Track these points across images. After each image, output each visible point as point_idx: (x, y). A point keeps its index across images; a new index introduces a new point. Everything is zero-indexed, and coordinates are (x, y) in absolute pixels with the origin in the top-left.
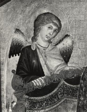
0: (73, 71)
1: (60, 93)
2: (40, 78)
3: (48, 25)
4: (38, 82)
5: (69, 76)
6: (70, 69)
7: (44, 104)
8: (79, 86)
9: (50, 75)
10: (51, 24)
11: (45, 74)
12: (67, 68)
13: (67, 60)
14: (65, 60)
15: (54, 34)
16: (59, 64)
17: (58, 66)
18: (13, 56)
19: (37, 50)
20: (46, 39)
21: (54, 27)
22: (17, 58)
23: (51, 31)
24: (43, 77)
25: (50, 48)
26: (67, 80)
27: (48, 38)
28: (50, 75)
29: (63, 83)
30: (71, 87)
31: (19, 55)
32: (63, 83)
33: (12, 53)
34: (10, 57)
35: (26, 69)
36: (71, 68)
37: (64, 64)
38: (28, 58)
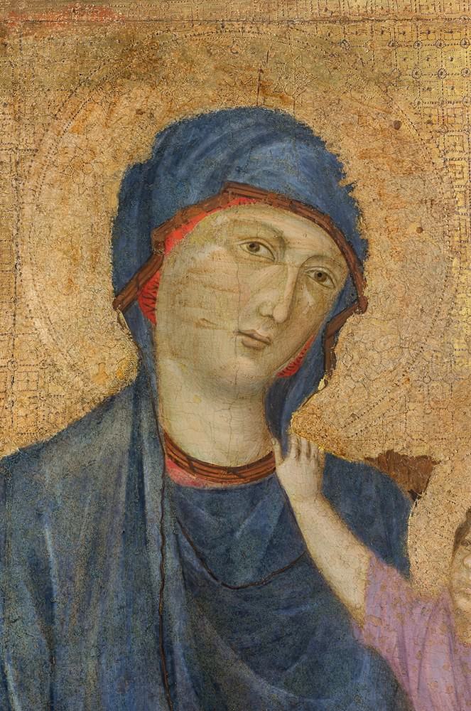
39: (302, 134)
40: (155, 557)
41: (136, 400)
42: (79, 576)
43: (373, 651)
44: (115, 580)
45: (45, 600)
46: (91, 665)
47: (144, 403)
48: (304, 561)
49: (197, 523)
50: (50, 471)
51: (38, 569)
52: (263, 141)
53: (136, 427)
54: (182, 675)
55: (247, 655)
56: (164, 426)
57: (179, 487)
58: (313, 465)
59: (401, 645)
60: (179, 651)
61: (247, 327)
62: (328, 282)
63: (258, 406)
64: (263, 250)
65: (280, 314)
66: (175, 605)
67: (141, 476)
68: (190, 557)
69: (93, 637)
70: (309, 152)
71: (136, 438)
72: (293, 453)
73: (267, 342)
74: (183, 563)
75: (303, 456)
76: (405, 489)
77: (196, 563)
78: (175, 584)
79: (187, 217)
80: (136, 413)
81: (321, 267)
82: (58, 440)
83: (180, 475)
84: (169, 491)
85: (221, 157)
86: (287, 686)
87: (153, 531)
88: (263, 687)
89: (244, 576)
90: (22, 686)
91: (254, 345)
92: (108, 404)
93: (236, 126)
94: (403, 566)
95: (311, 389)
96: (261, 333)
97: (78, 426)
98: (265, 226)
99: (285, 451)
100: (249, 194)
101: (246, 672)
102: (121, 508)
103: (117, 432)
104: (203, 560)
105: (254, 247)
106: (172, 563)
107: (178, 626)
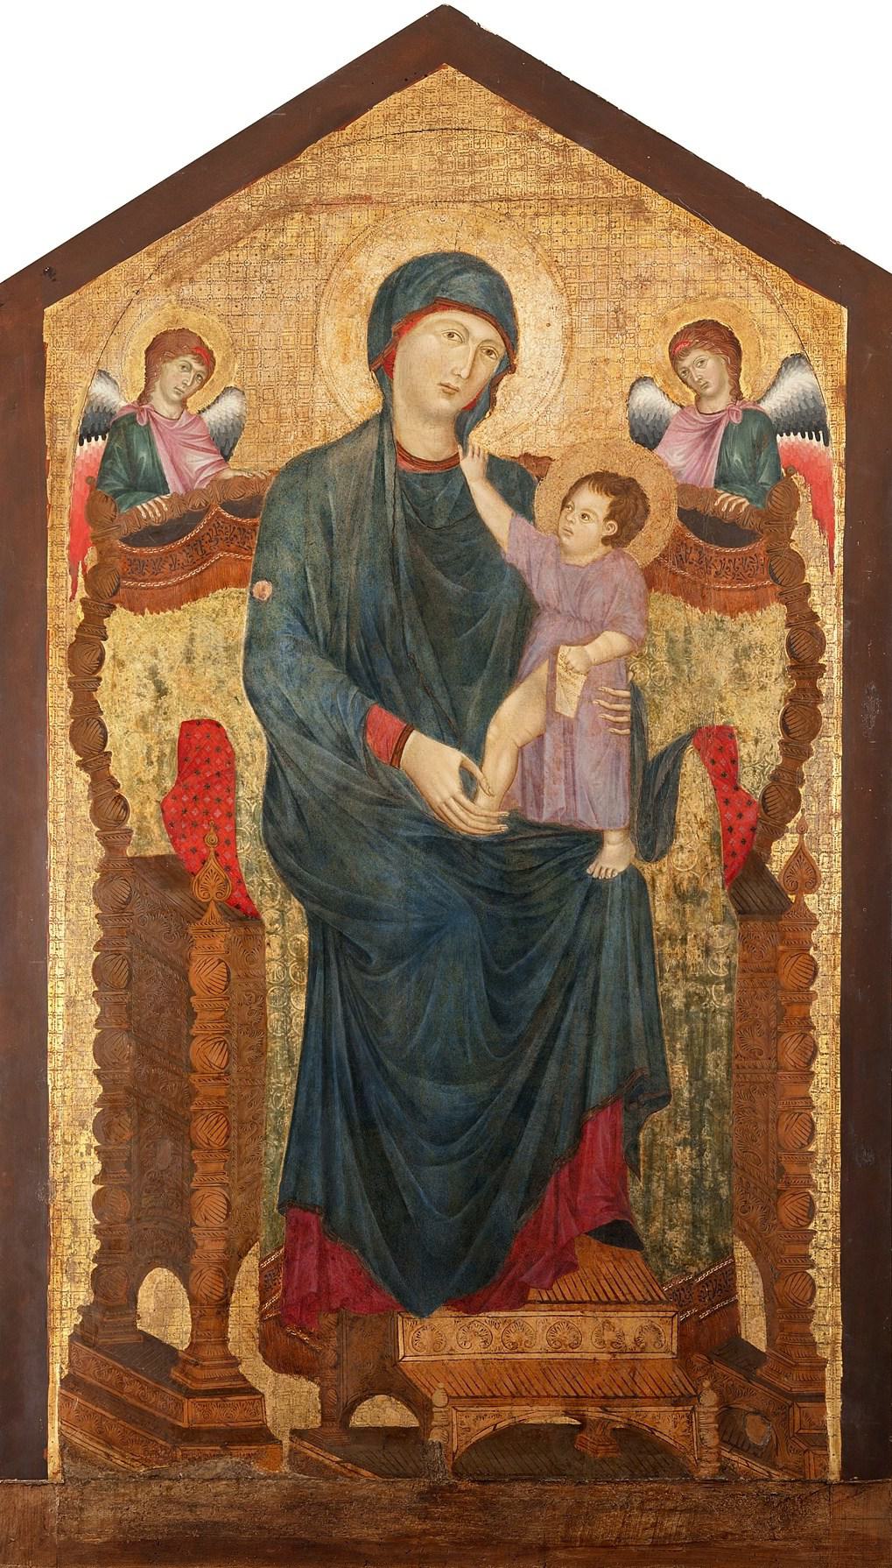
0: (245, 483)
1: (207, 538)
2: (157, 499)
3: (180, 361)
4: (152, 509)
5: (235, 495)
6: (235, 477)
7: (167, 566)
8: (258, 520)
9: (181, 491)
10: (189, 358)
11: (170, 486)
12: (228, 474)
13: (227, 453)
14: (222, 454)
15: (196, 384)
16: (208, 462)
17: (204, 468)
18: (89, 441)
19: (152, 426)
20: (175, 397)
21: (197, 367)
22: (99, 444)
23: (188, 377)
24: (164, 497)
25: (184, 420)
26: (227, 506)
27: (177, 393)
28: (181, 491)
29: (218, 514)
30: (236, 522)
31: (104, 438)
32: (218, 514)
33: (85, 435)
34: (81, 444)
35: (124, 475)
36: (239, 474)
37: (219, 463)
38: (128, 447)
39: (481, 267)
40: (390, 511)
41: (381, 423)
42: (348, 519)
43: (512, 566)
44: (367, 523)
45: (328, 533)
46: (353, 569)
47: (385, 424)
48: (474, 515)
49: (414, 493)
50: (332, 461)
51: (325, 515)
52: (457, 273)
53: (381, 438)
54: (403, 576)
55: (440, 566)
56: (397, 437)
57: (404, 472)
58: (481, 460)
59: (529, 562)
60: (402, 563)
61: (446, 381)
62: (493, 356)
63: (450, 427)
64: (456, 337)
65: (465, 373)
66: (401, 537)
67: (383, 465)
68: (410, 511)
69: (354, 554)
70: (485, 279)
71: (380, 444)
72: (470, 454)
73: (457, 390)
74: (406, 514)
75: (475, 456)
76: (533, 473)
77: (413, 515)
78: (401, 526)
79: (413, 318)
80: (381, 430)
81: (488, 346)
82: (338, 444)
83: (404, 465)
84: (398, 474)
85: (433, 282)
86: (463, 584)
87: (389, 496)
88: (449, 584)
89: (440, 522)
90: (315, 580)
91: (449, 391)
92: (365, 425)
93: (442, 264)
94: (531, 517)
95: (481, 418)
96: (453, 384)
97: (347, 436)
98: (458, 323)
99: (465, 452)
100: (447, 305)
101: (440, 576)
102: (371, 483)
103: (370, 440)
104: (417, 513)
105: (450, 335)
106: (399, 514)
107: (402, 549)
